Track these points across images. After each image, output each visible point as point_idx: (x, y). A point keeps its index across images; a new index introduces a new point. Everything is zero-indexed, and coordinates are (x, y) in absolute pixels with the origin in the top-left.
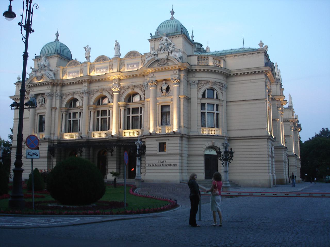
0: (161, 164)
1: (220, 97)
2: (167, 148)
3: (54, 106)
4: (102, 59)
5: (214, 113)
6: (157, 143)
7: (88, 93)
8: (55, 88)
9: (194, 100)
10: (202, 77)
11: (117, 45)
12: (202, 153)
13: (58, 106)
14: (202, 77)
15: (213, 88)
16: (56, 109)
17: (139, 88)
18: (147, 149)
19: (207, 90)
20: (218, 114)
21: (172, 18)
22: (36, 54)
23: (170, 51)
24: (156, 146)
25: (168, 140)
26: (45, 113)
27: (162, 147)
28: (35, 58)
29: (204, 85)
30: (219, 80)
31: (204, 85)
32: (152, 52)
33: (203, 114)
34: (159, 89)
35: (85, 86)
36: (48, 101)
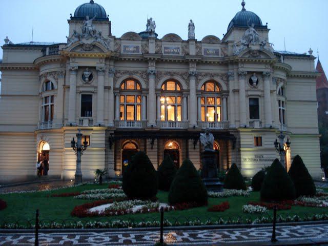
0: (258, 159)
3: (107, 85)
4: (172, 38)
7: (154, 74)
8: (108, 63)
11: (191, 26)
13: (111, 85)
16: (109, 88)
17: (219, 77)
21: (244, 10)
22: (71, 14)
23: (263, 44)
24: (251, 140)
25: (264, 134)
26: (92, 92)
27: (258, 142)
28: (70, 19)
32: (244, 41)
34: (247, 81)
35: (152, 66)
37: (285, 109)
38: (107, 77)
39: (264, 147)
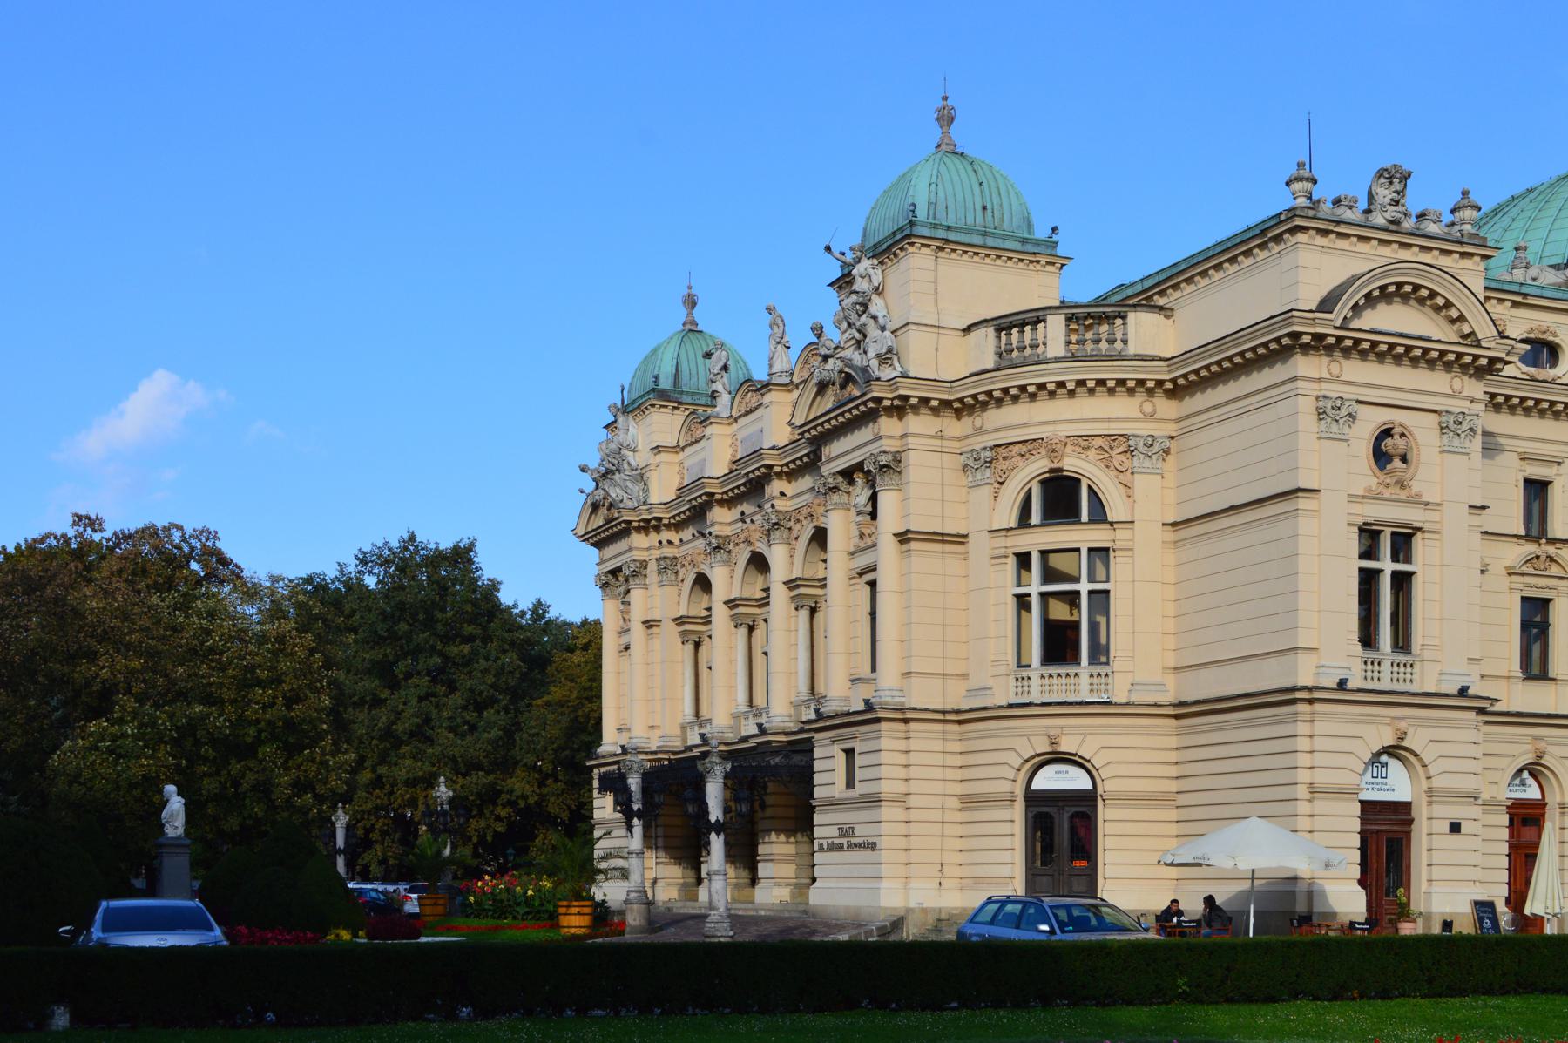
1: (1115, 511)
2: (859, 774)
5: (1078, 593)
6: (837, 750)
9: (980, 546)
10: (1005, 429)
12: (1005, 787)
14: (1005, 429)
15: (1061, 470)
18: (817, 779)
19: (1042, 482)
20: (1101, 598)
29: (1021, 464)
30: (1106, 425)
31: (1021, 464)
33: (1023, 602)
36: (636, 595)
37: (1084, 587)
38: (654, 589)
39: (860, 789)
